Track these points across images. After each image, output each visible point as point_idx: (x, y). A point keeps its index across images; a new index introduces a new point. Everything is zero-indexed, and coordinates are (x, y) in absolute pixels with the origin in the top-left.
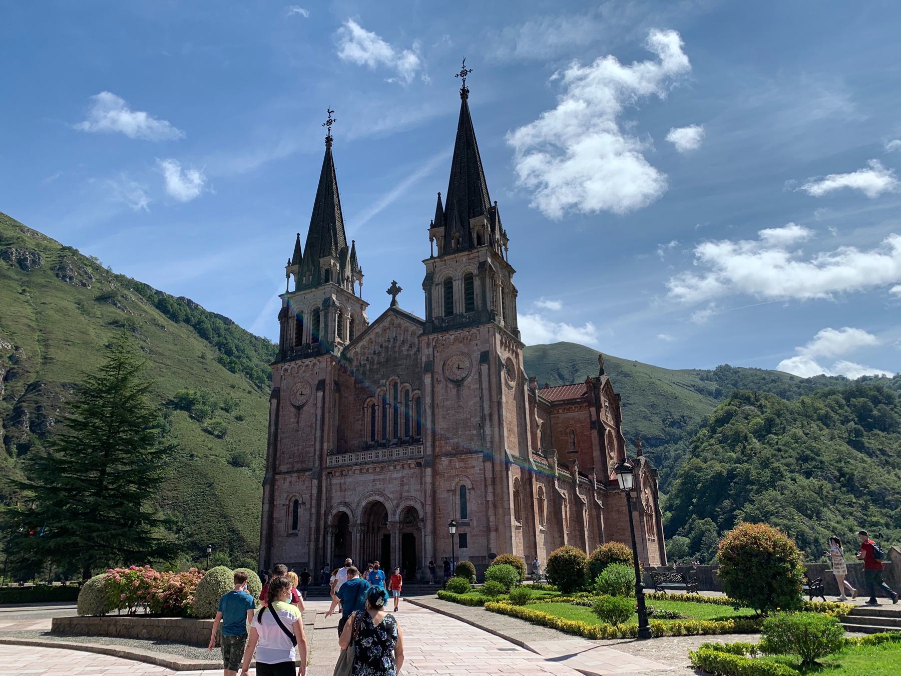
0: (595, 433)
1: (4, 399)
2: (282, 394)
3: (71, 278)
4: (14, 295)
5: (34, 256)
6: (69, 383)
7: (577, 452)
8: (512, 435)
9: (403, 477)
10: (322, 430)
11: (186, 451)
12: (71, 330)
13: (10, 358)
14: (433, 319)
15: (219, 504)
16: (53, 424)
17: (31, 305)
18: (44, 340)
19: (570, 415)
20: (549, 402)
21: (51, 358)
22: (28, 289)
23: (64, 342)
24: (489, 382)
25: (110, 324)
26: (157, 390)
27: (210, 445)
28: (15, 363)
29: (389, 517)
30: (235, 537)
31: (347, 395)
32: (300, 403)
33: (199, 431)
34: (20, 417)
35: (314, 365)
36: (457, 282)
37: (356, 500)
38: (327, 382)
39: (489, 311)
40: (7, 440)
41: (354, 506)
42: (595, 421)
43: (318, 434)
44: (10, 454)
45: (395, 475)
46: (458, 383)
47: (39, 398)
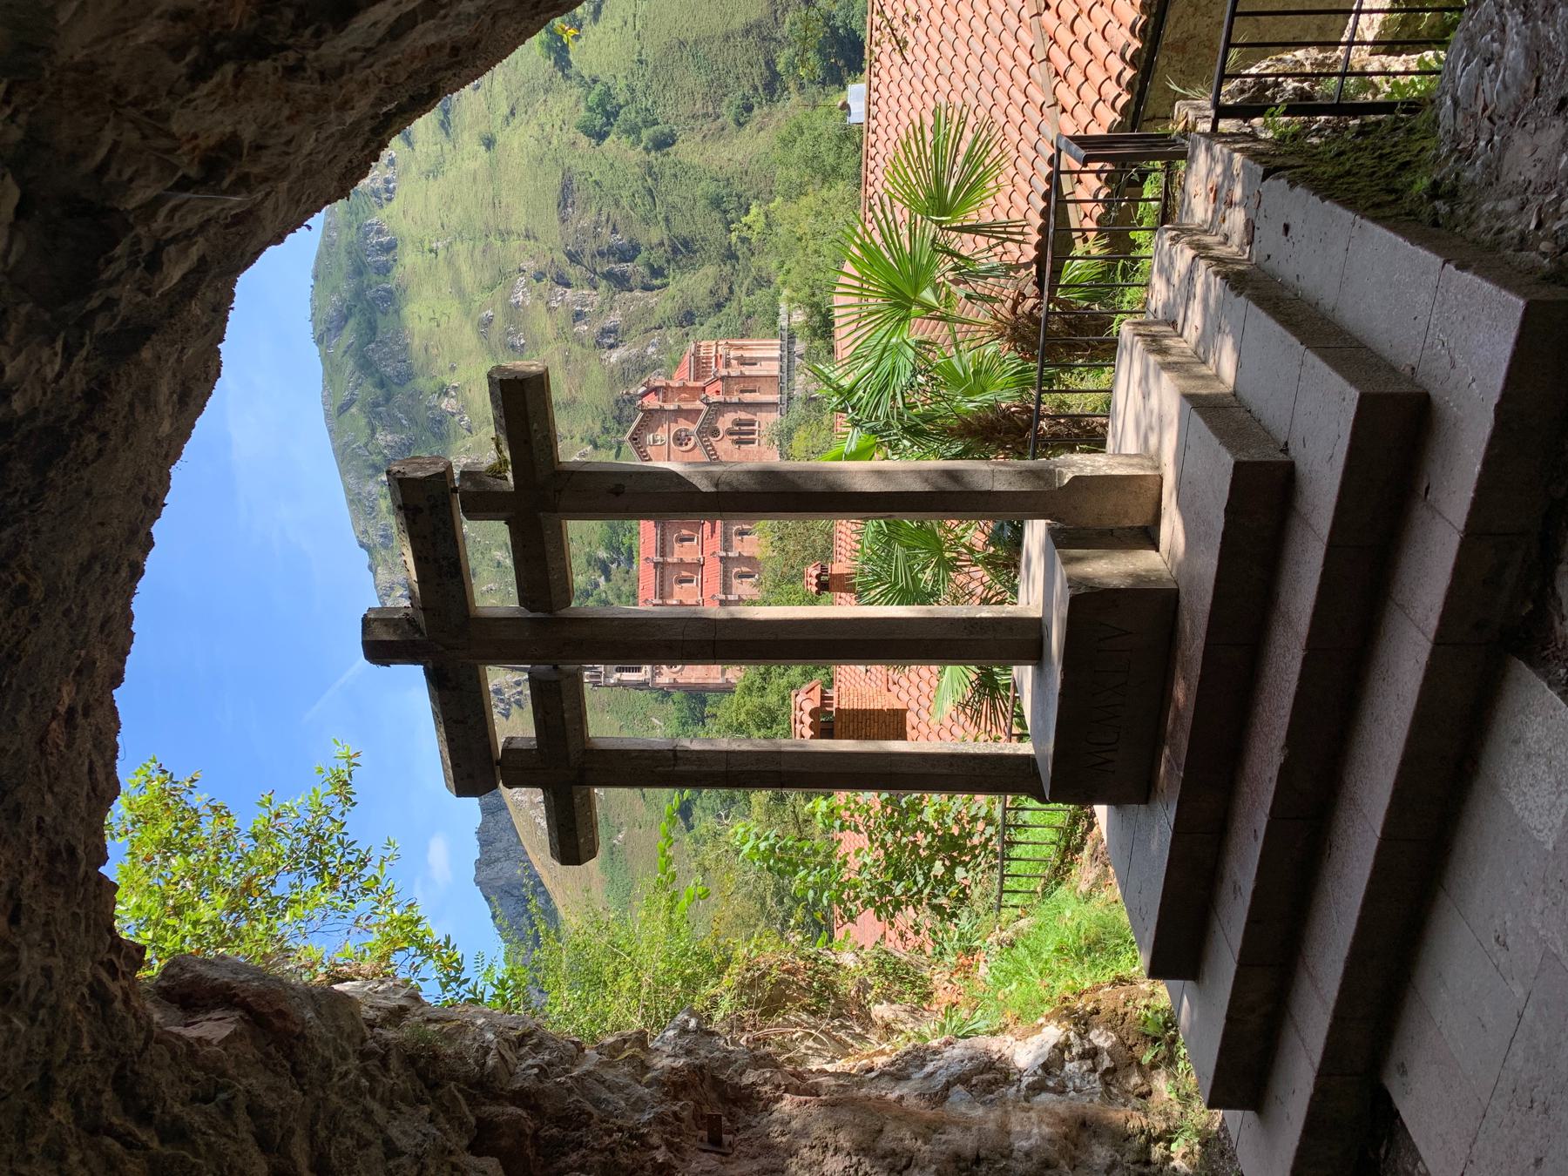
1: (595, 288)
3: (387, 181)
4: (441, 264)
5: (370, 232)
6: (560, 213)
11: (635, 67)
12: (476, 195)
13: (538, 280)
15: (710, 39)
16: (618, 236)
17: (451, 243)
18: (501, 234)
21: (527, 230)
22: (427, 248)
23: (497, 209)
25: (447, 134)
26: (542, 81)
27: (618, 23)
28: (545, 275)
30: (755, 32)
33: (599, 28)
34: (615, 274)
40: (647, 288)
44: (665, 285)
47: (587, 252)
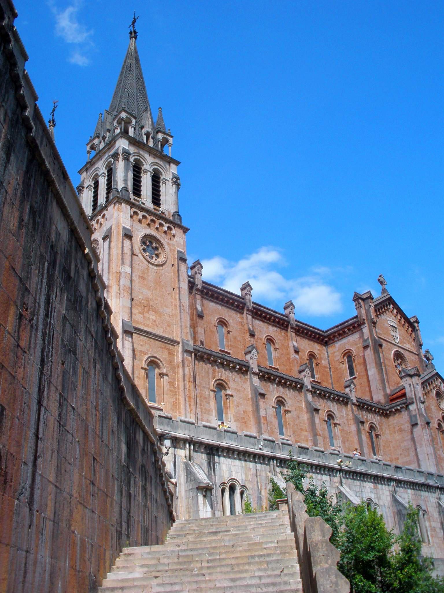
0: (369, 353)
7: (355, 378)
8: (151, 312)
19: (344, 341)
20: (323, 331)
24: (109, 254)
36: (101, 177)
42: (368, 338)
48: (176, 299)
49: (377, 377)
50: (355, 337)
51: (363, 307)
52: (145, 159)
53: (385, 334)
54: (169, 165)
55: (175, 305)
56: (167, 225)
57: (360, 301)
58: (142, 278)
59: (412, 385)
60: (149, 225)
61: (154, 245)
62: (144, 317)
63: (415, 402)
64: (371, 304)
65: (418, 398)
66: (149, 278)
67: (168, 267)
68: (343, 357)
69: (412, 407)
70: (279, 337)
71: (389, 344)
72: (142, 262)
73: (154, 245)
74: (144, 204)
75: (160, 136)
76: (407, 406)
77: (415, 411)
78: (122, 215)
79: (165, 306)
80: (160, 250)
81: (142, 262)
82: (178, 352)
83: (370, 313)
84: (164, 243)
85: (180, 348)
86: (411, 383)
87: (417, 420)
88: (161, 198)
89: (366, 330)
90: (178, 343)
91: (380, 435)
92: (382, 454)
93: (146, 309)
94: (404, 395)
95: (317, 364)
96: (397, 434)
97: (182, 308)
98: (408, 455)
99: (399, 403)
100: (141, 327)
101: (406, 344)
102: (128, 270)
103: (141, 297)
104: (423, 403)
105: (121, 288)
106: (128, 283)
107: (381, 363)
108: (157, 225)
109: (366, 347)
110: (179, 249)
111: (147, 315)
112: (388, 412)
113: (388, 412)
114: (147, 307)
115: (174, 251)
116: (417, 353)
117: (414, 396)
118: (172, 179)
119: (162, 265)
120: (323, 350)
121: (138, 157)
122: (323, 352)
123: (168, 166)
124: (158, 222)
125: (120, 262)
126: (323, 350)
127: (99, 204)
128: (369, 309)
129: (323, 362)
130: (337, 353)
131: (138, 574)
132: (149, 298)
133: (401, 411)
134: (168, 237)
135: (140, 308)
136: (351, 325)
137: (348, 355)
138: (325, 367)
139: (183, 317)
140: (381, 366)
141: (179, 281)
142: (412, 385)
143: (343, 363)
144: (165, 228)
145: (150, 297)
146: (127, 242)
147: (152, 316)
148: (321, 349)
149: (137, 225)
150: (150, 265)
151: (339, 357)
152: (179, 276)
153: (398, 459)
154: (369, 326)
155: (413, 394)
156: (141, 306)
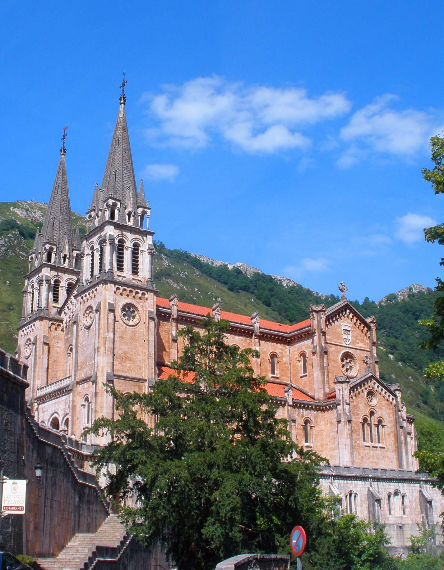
2: (22, 348)
7: (306, 376)
9: (66, 399)
10: (34, 372)
14: (84, 281)
19: (302, 343)
24: (99, 324)
29: (60, 427)
31: (59, 345)
32: (28, 355)
35: (34, 325)
37: (48, 418)
38: (38, 337)
39: (107, 271)
41: (46, 423)
42: (316, 346)
43: (32, 374)
45: (64, 398)
46: (88, 328)
48: (145, 348)
49: (320, 378)
50: (308, 342)
51: (316, 319)
52: (127, 238)
53: (336, 338)
54: (146, 237)
55: (145, 353)
56: (142, 292)
57: (314, 313)
58: (121, 337)
59: (341, 390)
60: (128, 296)
61: (132, 309)
62: (122, 366)
63: (341, 403)
64: (322, 316)
65: (344, 400)
66: (127, 337)
67: (141, 325)
68: (300, 357)
69: (339, 407)
70: (244, 344)
71: (338, 347)
72: (122, 326)
73: (132, 309)
74: (125, 277)
75: (140, 210)
76: (337, 406)
77: (341, 410)
78: (107, 293)
79: (138, 355)
80: (136, 312)
81: (122, 326)
82: (145, 386)
83: (321, 324)
84: (139, 306)
85: (146, 384)
86: (341, 388)
87: (341, 418)
88: (139, 267)
89: (316, 338)
90: (146, 380)
91: (314, 427)
92: (314, 442)
93: (124, 360)
94: (335, 397)
95: (278, 362)
96: (328, 426)
97: (149, 355)
98: (334, 443)
99: (332, 402)
100: (120, 374)
101: (358, 343)
102: (111, 335)
103: (120, 352)
104: (348, 404)
105: (107, 350)
106: (112, 346)
107: (324, 367)
108: (134, 294)
109: (314, 353)
110: (150, 309)
111: (124, 364)
112: (324, 408)
113: (324, 408)
114: (125, 358)
115: (146, 311)
116: (369, 350)
117: (341, 399)
118: (148, 250)
119: (137, 325)
120: (286, 348)
121: (121, 238)
122: (286, 350)
123: (145, 238)
124: (135, 291)
125: (106, 330)
126: (286, 348)
127: (94, 275)
128: (320, 321)
129: (284, 359)
130: (296, 353)
131: (77, 544)
132: (126, 352)
133: (333, 409)
134: (142, 301)
135: (119, 360)
136: (306, 332)
137: (303, 355)
138: (286, 363)
139: (149, 362)
140: (324, 370)
141: (148, 335)
142: (341, 390)
143: (299, 361)
144: (140, 295)
145: (127, 350)
146: (111, 315)
147: (128, 365)
148: (283, 348)
149: (119, 297)
150: (128, 327)
151: (297, 356)
152: (148, 331)
153: (327, 445)
154: (319, 335)
155: (341, 397)
156: (120, 359)
